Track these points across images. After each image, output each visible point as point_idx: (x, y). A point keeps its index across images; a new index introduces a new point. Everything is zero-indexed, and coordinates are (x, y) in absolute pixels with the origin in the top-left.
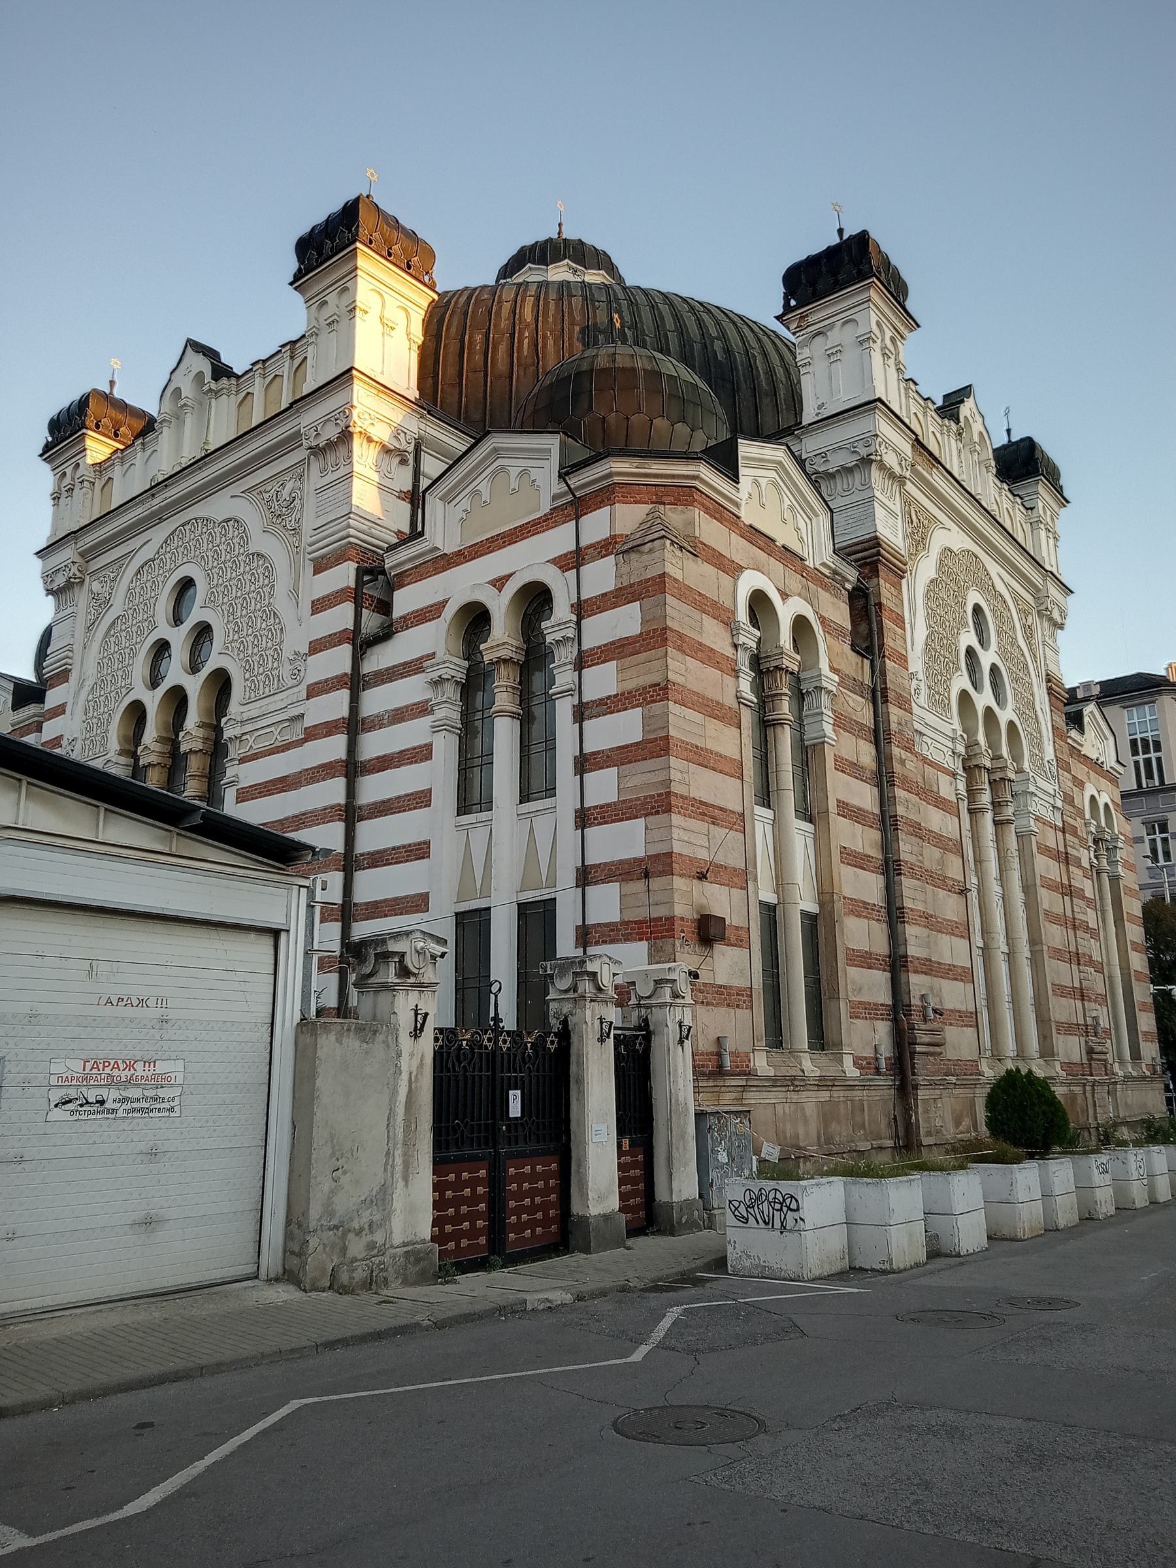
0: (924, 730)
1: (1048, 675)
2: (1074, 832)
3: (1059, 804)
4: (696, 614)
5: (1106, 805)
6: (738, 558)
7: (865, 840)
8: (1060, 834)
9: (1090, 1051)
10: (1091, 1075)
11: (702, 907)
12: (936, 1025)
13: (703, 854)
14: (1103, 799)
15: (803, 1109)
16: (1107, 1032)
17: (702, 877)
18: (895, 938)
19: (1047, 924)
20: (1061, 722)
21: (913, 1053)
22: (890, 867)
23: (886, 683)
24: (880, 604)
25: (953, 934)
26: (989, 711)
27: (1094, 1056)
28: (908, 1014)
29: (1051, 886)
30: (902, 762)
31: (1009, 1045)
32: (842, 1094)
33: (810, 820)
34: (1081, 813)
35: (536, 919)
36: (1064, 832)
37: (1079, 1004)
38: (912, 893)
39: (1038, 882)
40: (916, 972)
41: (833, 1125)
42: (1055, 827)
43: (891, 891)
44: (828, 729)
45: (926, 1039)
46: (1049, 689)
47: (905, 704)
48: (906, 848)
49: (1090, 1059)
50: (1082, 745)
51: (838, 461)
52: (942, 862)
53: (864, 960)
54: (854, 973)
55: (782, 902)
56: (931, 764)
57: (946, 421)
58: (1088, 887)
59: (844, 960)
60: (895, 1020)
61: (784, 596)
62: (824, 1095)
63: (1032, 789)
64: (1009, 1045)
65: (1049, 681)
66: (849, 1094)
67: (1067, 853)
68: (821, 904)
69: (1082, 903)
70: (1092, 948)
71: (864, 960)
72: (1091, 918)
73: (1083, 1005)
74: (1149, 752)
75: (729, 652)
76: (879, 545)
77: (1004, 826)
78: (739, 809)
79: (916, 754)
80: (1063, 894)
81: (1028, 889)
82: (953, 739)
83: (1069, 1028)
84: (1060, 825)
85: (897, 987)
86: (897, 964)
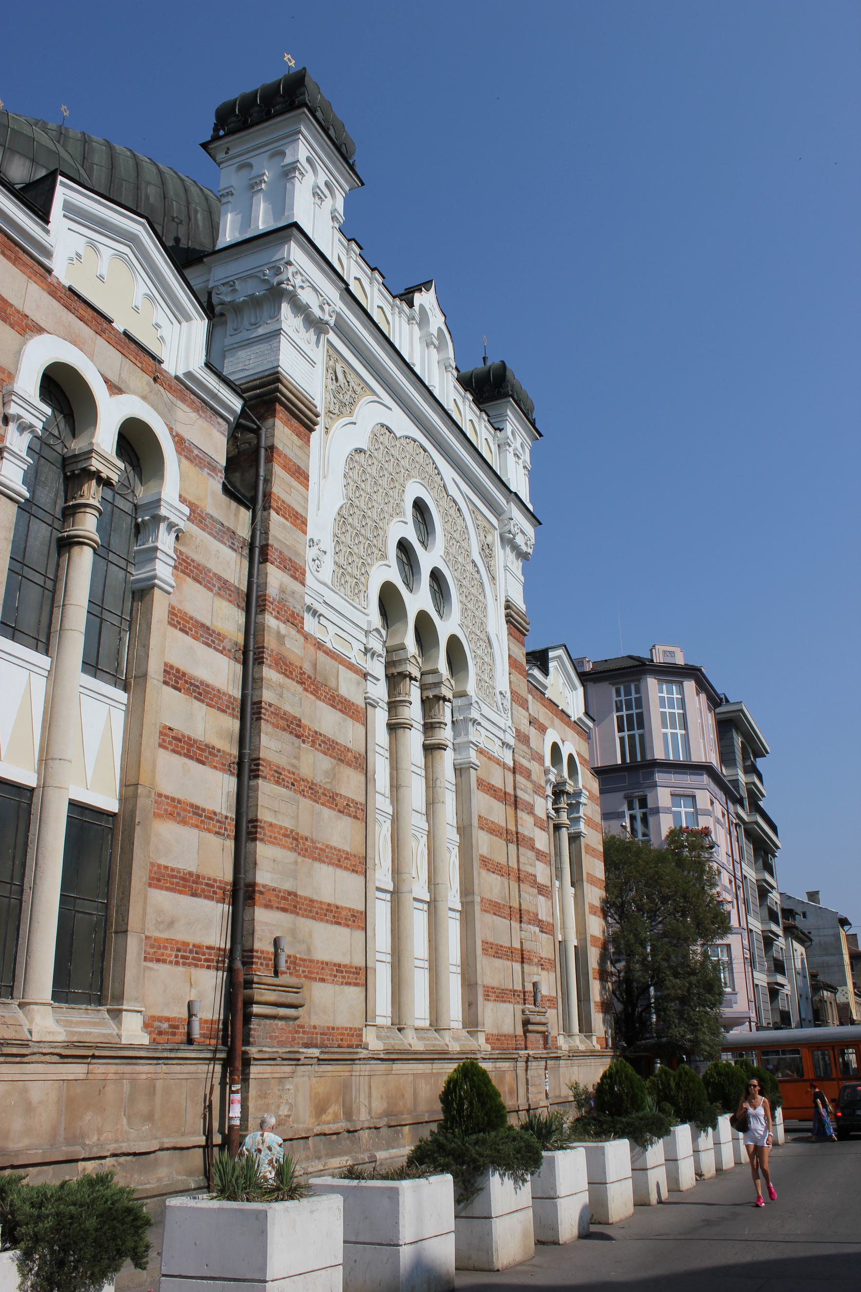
0: (321, 609)
1: (507, 601)
2: (528, 775)
3: (512, 741)
5: (571, 757)
7: (217, 728)
8: (509, 776)
9: (526, 1023)
10: (526, 1048)
14: (566, 750)
15: (26, 1090)
16: (552, 1001)
18: (242, 862)
19: (484, 873)
21: (248, 1018)
22: (247, 768)
23: (267, 539)
24: (271, 448)
25: (340, 867)
26: (423, 618)
27: (531, 1027)
28: (248, 962)
29: (493, 829)
30: (280, 638)
31: (419, 1011)
32: (113, 1069)
33: (126, 689)
34: (540, 759)
36: (514, 773)
37: (517, 966)
38: (272, 803)
39: (475, 822)
40: (268, 906)
41: (88, 1116)
42: (504, 766)
43: (244, 799)
44: (163, 570)
45: (271, 997)
48: (272, 745)
49: (526, 1031)
50: (546, 688)
51: (245, 290)
52: (333, 775)
53: (190, 884)
54: (163, 900)
55: (44, 785)
56: (328, 653)
57: (398, 301)
58: (542, 840)
59: (145, 879)
60: (231, 971)
62: (77, 1070)
63: (474, 714)
64: (419, 1011)
65: (507, 607)
66: (128, 1069)
67: (516, 796)
68: (123, 800)
69: (531, 855)
70: (542, 907)
71: (190, 884)
72: (542, 872)
73: (523, 968)
76: (278, 380)
77: (437, 753)
79: (307, 637)
80: (508, 841)
81: (464, 830)
82: (367, 633)
83: (501, 995)
84: (511, 764)
85: (239, 928)
86: (242, 894)
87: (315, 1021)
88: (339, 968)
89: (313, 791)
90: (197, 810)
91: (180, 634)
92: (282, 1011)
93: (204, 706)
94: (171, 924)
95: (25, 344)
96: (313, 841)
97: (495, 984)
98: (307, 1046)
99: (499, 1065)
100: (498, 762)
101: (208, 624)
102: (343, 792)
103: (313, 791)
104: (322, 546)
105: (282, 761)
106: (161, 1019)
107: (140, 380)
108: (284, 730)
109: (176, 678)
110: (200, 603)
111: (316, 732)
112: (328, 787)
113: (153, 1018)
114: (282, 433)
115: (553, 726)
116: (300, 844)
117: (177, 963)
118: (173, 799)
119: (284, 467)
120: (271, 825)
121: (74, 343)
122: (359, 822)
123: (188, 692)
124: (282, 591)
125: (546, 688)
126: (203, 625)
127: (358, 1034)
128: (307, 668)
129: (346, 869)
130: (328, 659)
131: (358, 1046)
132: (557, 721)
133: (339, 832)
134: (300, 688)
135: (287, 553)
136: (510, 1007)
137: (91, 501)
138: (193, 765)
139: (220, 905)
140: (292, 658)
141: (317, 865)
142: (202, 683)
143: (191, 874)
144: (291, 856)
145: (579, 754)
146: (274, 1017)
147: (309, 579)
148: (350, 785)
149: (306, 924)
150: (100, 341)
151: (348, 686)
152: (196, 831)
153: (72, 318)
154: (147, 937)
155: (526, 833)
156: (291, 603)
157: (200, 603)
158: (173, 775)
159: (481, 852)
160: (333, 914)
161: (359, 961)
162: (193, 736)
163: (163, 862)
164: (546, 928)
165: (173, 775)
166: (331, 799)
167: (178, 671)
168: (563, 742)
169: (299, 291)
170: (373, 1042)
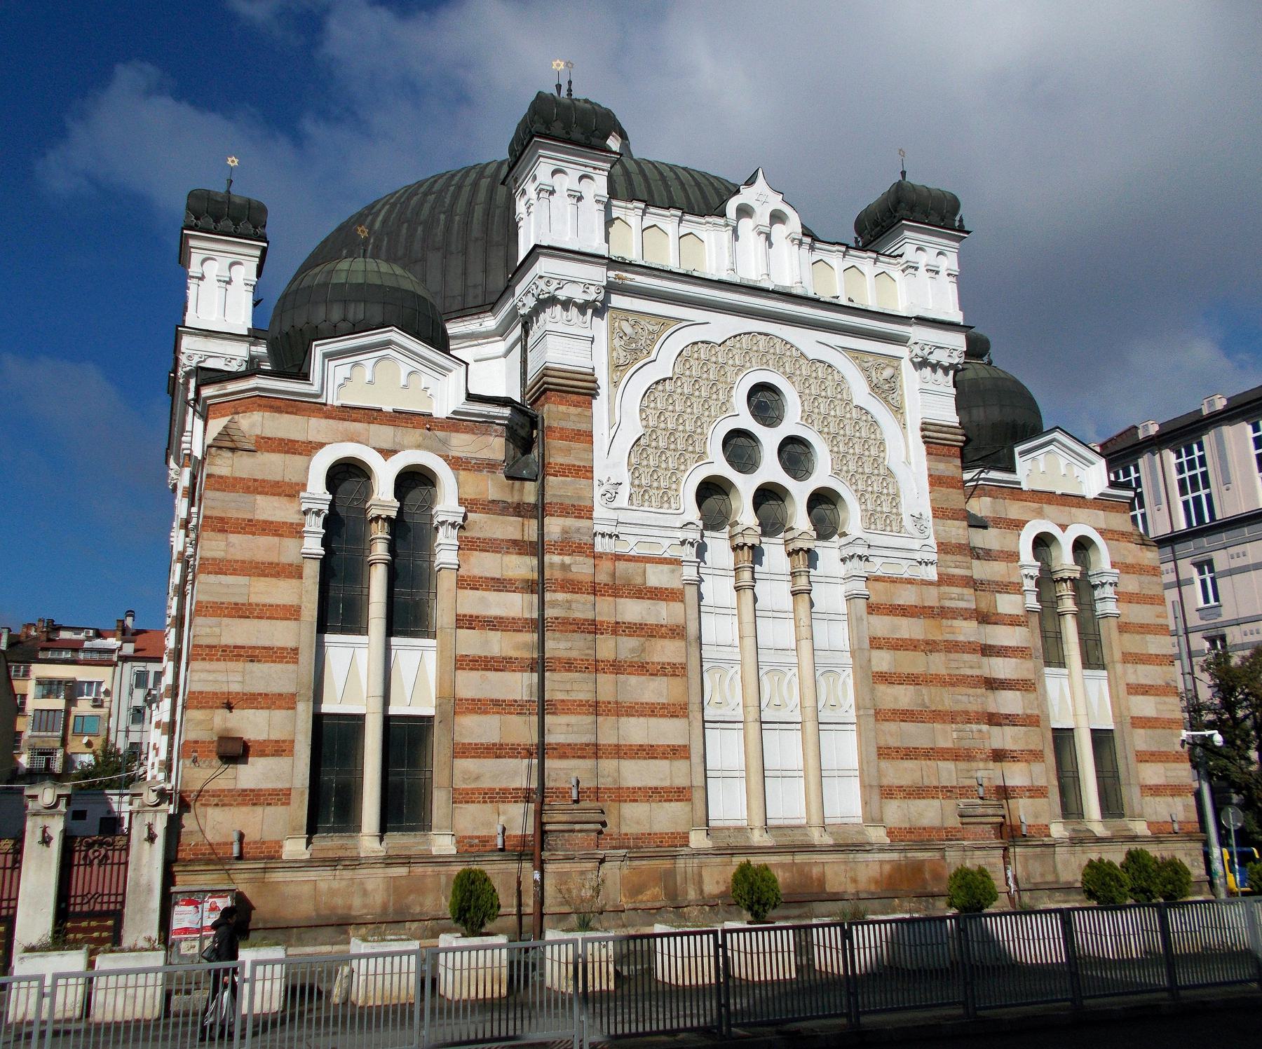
3: (934, 557)
4: (248, 498)
6: (313, 437)
11: (227, 730)
12: (595, 804)
13: (235, 688)
17: (229, 707)
19: (882, 688)
20: (951, 467)
21: (543, 833)
30: (565, 567)
32: (430, 869)
34: (1013, 556)
35: (1055, 658)
40: (563, 756)
46: (923, 437)
47: (585, 512)
50: (1019, 483)
54: (466, 765)
59: (449, 752)
61: (387, 453)
62: (402, 871)
65: (922, 430)
66: (441, 869)
70: (1010, 702)
72: (1002, 668)
74: (1195, 468)
75: (293, 518)
78: (291, 644)
83: (918, 792)
87: (625, 830)
88: (655, 790)
89: (617, 667)
90: (497, 703)
91: (472, 592)
92: (577, 827)
93: (499, 633)
94: (477, 778)
95: (310, 460)
96: (617, 703)
97: (905, 781)
98: (615, 848)
99: (909, 855)
100: (910, 581)
101: (498, 576)
102: (656, 660)
103: (617, 667)
104: (613, 481)
105: (574, 654)
106: (470, 837)
107: (416, 435)
108: (574, 631)
109: (466, 622)
110: (486, 564)
111: (617, 623)
112: (636, 659)
113: (465, 837)
114: (554, 413)
115: (1040, 514)
116: (595, 708)
117: (485, 802)
118: (473, 700)
119: (561, 438)
120: (563, 701)
121: (352, 440)
122: (678, 679)
123: (482, 628)
124: (565, 531)
125: (1019, 483)
126: (493, 579)
127: (685, 837)
128: (603, 578)
129: (661, 716)
130: (632, 564)
131: (681, 846)
132: (1049, 509)
133: (653, 690)
134: (591, 597)
135: (568, 502)
136: (936, 803)
137: (380, 535)
138: (491, 675)
139: (526, 761)
140: (580, 578)
141: (623, 719)
142: (496, 618)
143: (494, 745)
144: (591, 718)
145: (1102, 532)
146: (572, 831)
147: (599, 511)
148: (667, 651)
149: (608, 765)
150: (374, 428)
151: (657, 577)
152: (497, 716)
153: (346, 423)
154: (454, 789)
155: (961, 638)
156: (576, 538)
157: (486, 564)
158: (471, 685)
159: (875, 669)
160: (648, 752)
161: (681, 781)
162: (489, 655)
163: (466, 741)
164: (1031, 721)
165: (471, 685)
166: (642, 668)
167: (471, 616)
168: (1064, 527)
169: (557, 293)
170: (698, 840)
